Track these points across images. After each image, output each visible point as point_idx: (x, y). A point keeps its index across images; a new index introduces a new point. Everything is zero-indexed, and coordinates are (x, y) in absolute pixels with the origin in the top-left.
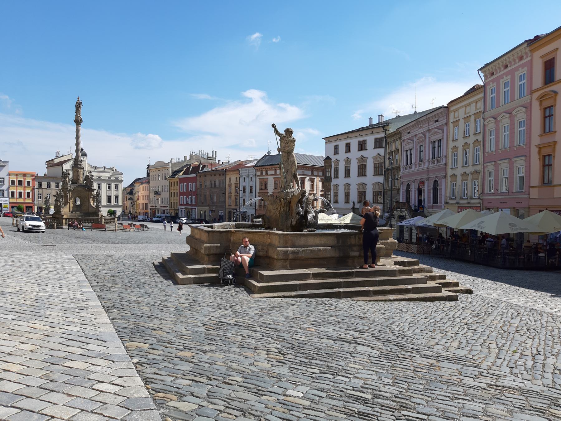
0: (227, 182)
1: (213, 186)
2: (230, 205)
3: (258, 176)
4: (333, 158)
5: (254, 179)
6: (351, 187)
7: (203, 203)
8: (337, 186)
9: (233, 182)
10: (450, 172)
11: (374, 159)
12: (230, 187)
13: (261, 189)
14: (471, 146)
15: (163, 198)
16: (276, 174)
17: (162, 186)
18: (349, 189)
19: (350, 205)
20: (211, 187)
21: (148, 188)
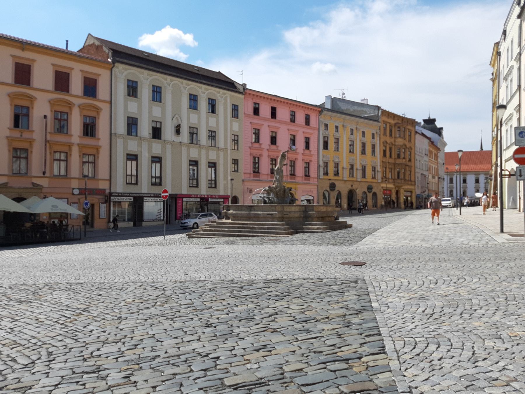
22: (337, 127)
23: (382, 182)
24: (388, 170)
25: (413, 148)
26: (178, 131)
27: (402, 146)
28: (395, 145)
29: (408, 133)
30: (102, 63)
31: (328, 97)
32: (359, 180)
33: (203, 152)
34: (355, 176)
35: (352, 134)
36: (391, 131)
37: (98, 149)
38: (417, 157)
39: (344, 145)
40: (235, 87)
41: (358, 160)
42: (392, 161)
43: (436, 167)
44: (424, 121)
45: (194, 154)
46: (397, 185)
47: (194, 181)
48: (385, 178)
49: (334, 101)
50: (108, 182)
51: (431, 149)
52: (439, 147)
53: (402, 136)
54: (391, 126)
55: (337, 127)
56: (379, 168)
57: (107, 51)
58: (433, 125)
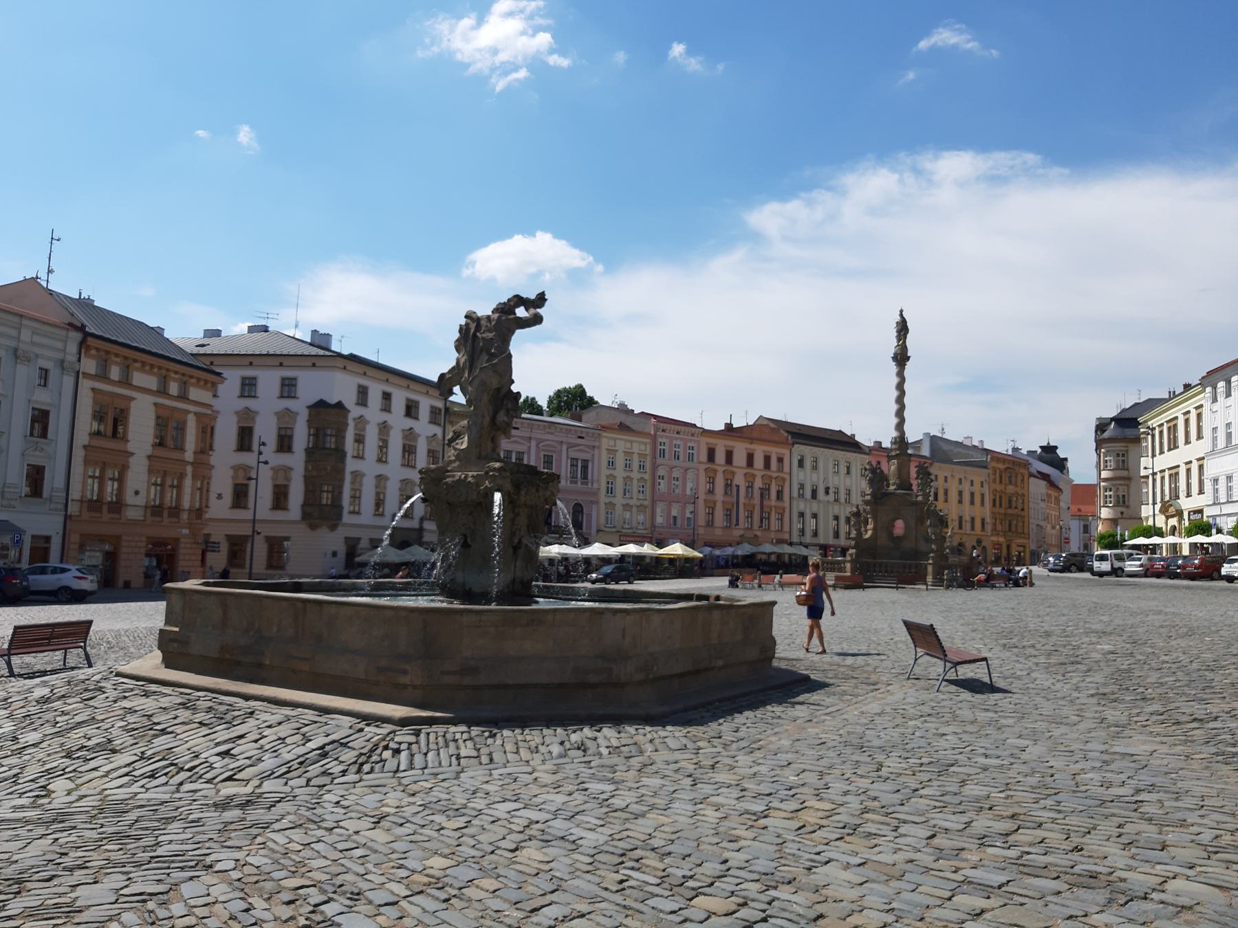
3: (87, 375)
4: (355, 411)
6: (389, 484)
8: (357, 475)
10: (603, 498)
11: (428, 441)
14: (635, 482)
22: (946, 478)
23: (992, 535)
24: (998, 522)
25: (1026, 494)
26: (827, 492)
27: (1014, 494)
28: (1006, 493)
29: (1020, 478)
30: (784, 443)
31: (927, 434)
32: (968, 532)
33: (842, 507)
34: (964, 527)
35: (960, 483)
36: (1001, 477)
37: (784, 509)
38: (1031, 505)
39: (953, 496)
40: (860, 448)
41: (967, 511)
42: (1002, 511)
43: (1058, 514)
44: (1041, 447)
45: (836, 510)
46: (1008, 538)
47: (837, 535)
48: (994, 529)
49: (934, 440)
50: (788, 535)
51: (1050, 492)
52: (1060, 487)
53: (1013, 482)
54: (1000, 472)
55: (946, 478)
56: (988, 520)
57: (786, 434)
58: (1053, 455)
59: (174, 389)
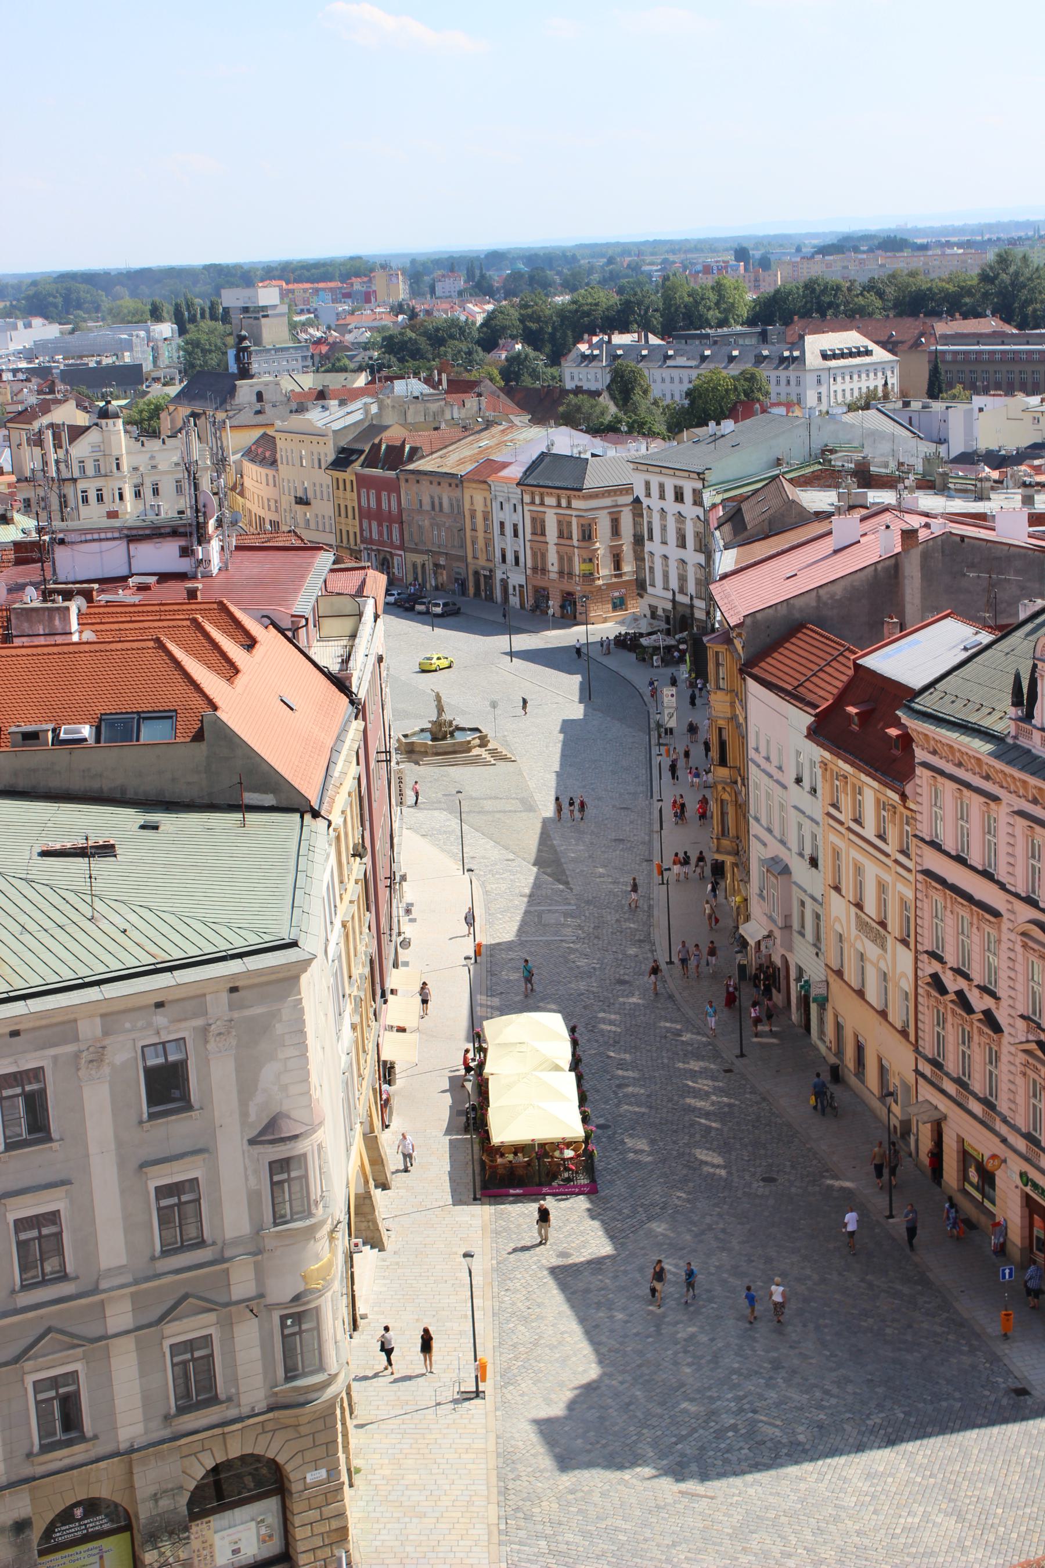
0: (467, 506)
1: (437, 508)
2: (475, 558)
5: (519, 508)
7: (416, 544)
9: (479, 507)
12: (473, 516)
13: (534, 533)
15: (320, 517)
16: (559, 505)
17: (314, 485)
18: (667, 566)
19: (669, 595)
20: (433, 508)
21: (275, 481)
59: (564, 503)
